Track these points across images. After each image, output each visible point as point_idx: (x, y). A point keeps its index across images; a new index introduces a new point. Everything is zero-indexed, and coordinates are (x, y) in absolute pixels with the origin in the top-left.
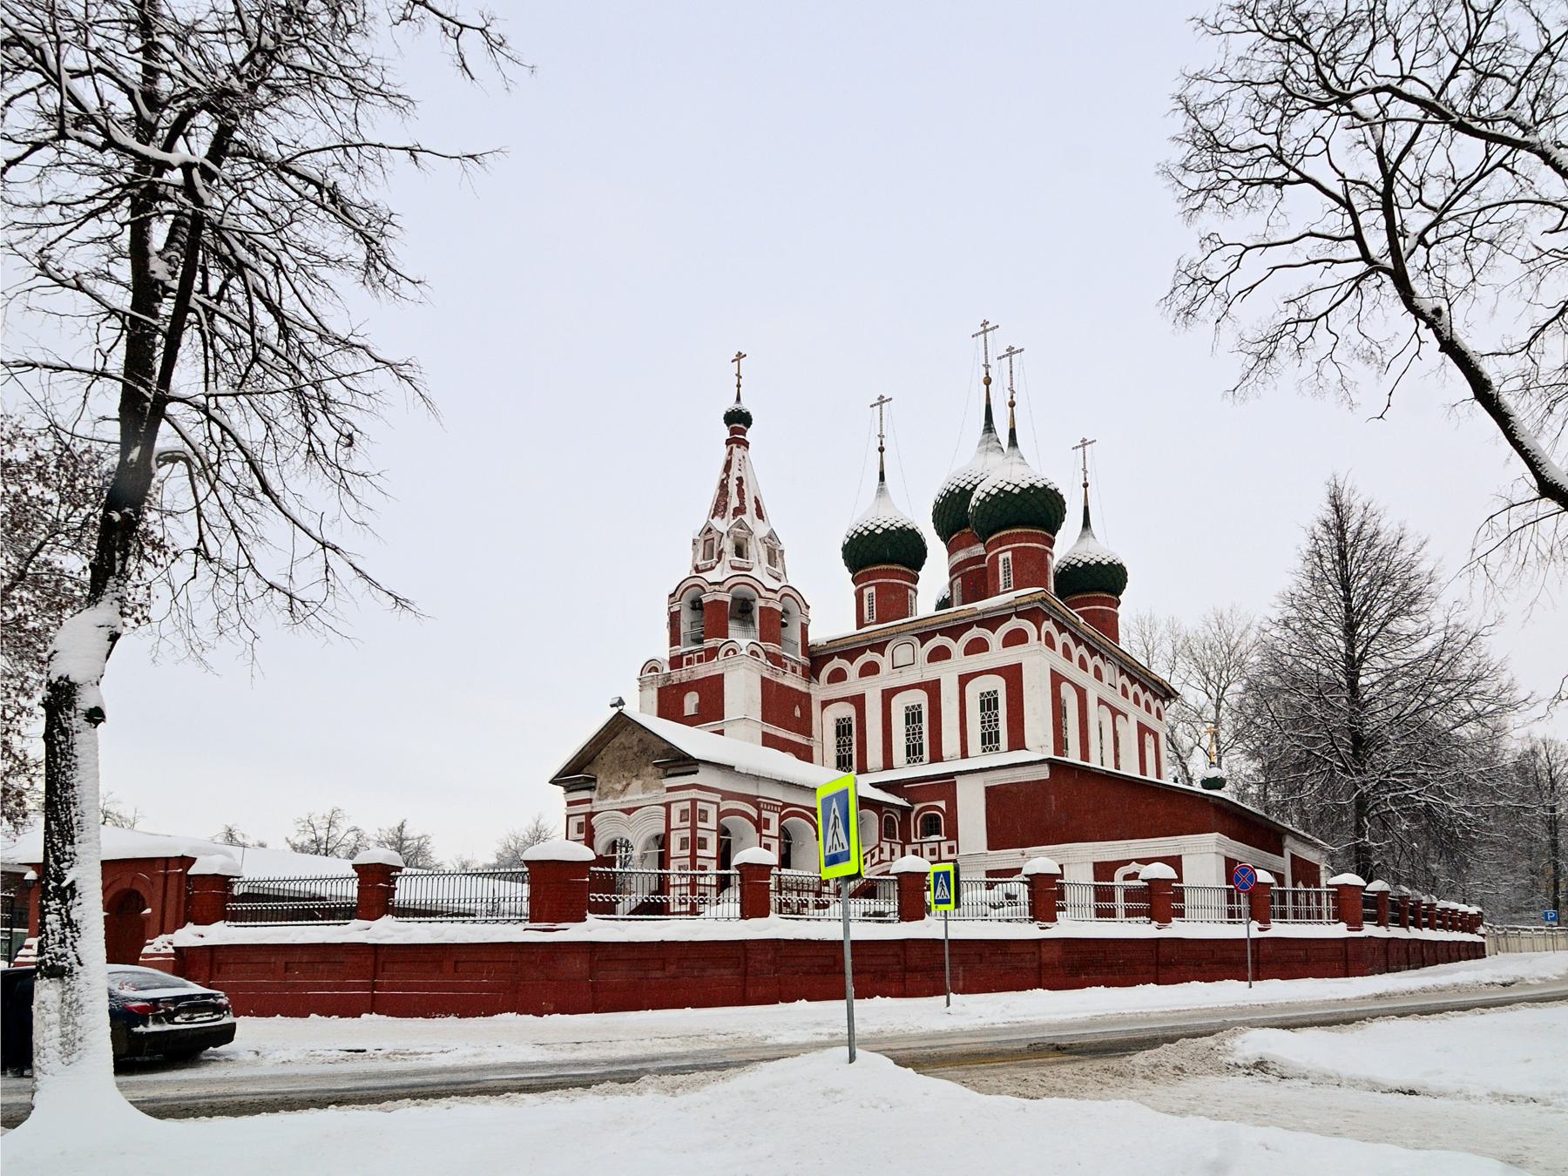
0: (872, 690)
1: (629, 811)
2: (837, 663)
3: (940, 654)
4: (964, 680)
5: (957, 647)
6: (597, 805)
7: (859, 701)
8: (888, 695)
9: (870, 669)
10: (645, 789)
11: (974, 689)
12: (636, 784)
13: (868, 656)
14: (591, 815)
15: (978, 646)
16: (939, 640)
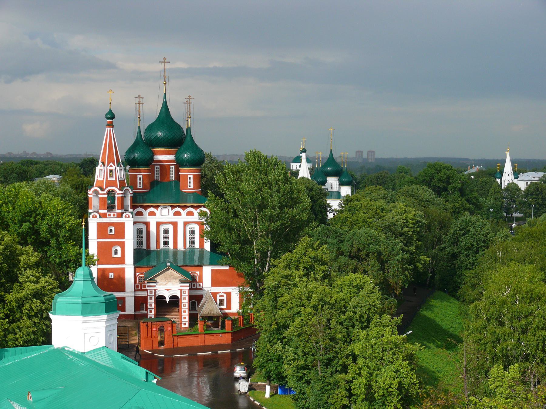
0: (153, 221)
1: (168, 290)
2: (139, 209)
3: (177, 214)
4: (186, 224)
5: (183, 212)
6: (157, 287)
7: (147, 224)
8: (159, 224)
9: (152, 214)
10: (173, 284)
11: (188, 228)
12: (169, 283)
13: (152, 209)
14: (155, 290)
15: (190, 214)
16: (178, 209)
